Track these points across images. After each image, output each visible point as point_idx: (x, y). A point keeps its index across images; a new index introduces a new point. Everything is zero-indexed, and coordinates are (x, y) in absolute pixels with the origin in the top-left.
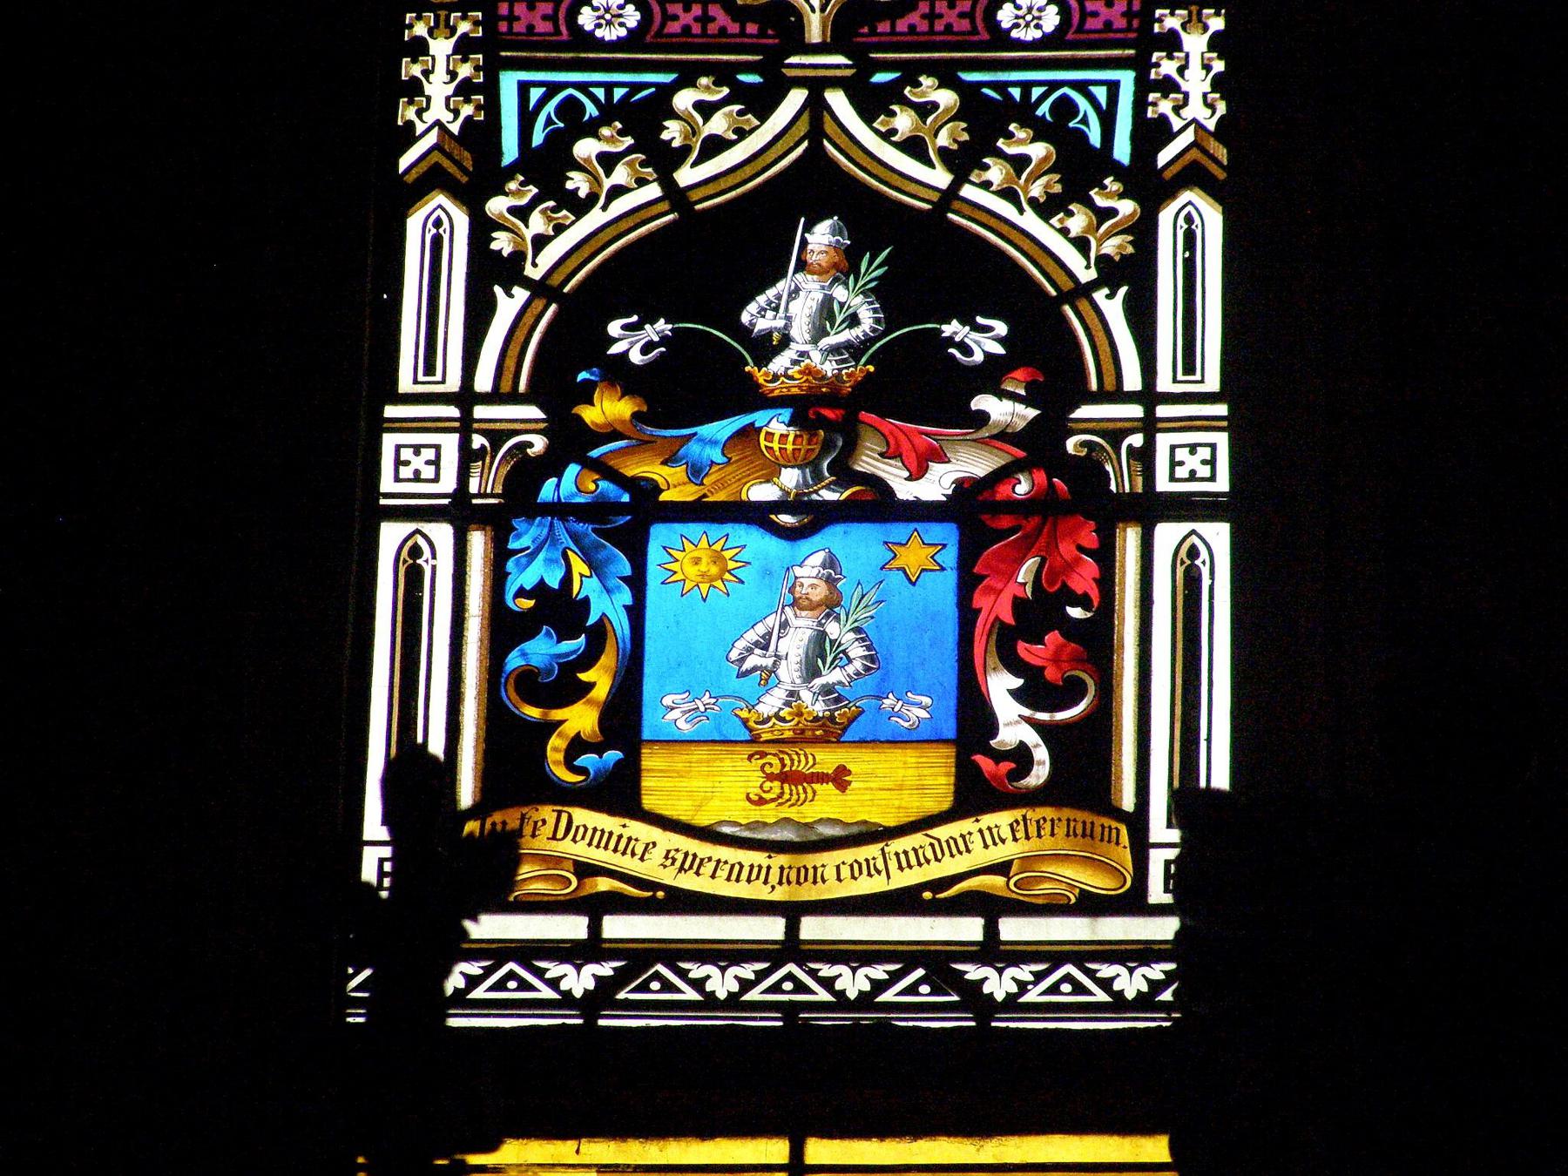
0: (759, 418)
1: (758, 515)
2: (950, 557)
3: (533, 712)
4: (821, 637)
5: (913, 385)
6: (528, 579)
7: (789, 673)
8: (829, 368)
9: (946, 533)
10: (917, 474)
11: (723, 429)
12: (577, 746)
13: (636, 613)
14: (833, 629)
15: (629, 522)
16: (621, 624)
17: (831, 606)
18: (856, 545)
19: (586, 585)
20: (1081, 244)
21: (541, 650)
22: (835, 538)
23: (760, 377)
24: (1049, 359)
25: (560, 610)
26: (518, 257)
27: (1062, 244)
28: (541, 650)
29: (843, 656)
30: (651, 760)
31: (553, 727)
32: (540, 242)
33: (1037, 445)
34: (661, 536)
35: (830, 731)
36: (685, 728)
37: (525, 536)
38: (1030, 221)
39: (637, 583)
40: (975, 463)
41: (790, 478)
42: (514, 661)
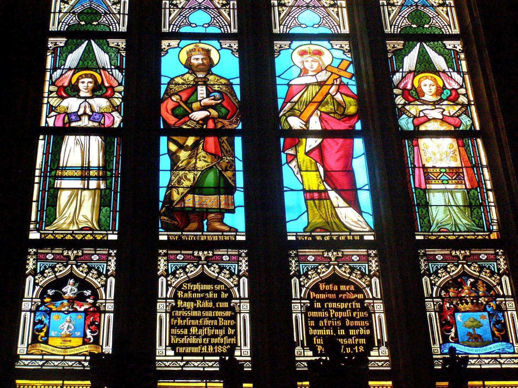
0: (64, 301)
1: (63, 312)
2: (83, 317)
3: (37, 333)
4: (69, 326)
5: (80, 298)
6: (38, 318)
7: (65, 329)
8: (72, 296)
9: (83, 314)
10: (80, 307)
11: (60, 302)
12: (42, 337)
13: (49, 322)
14: (70, 325)
15: (49, 312)
16: (48, 324)
17: (70, 322)
18: (73, 315)
19: (44, 319)
20: (99, 283)
21: (39, 326)
22: (71, 314)
23: (64, 296)
24: (95, 295)
25: (41, 322)
26: (38, 283)
27: (97, 283)
28: (39, 326)
29: (71, 328)
30: (50, 339)
31: (39, 335)
32: (41, 281)
33: (93, 305)
34: (52, 314)
35: (69, 336)
36: (53, 335)
37: (38, 314)
38: (94, 280)
39: (50, 319)
40: (86, 307)
41: (67, 308)
42: (36, 327)
